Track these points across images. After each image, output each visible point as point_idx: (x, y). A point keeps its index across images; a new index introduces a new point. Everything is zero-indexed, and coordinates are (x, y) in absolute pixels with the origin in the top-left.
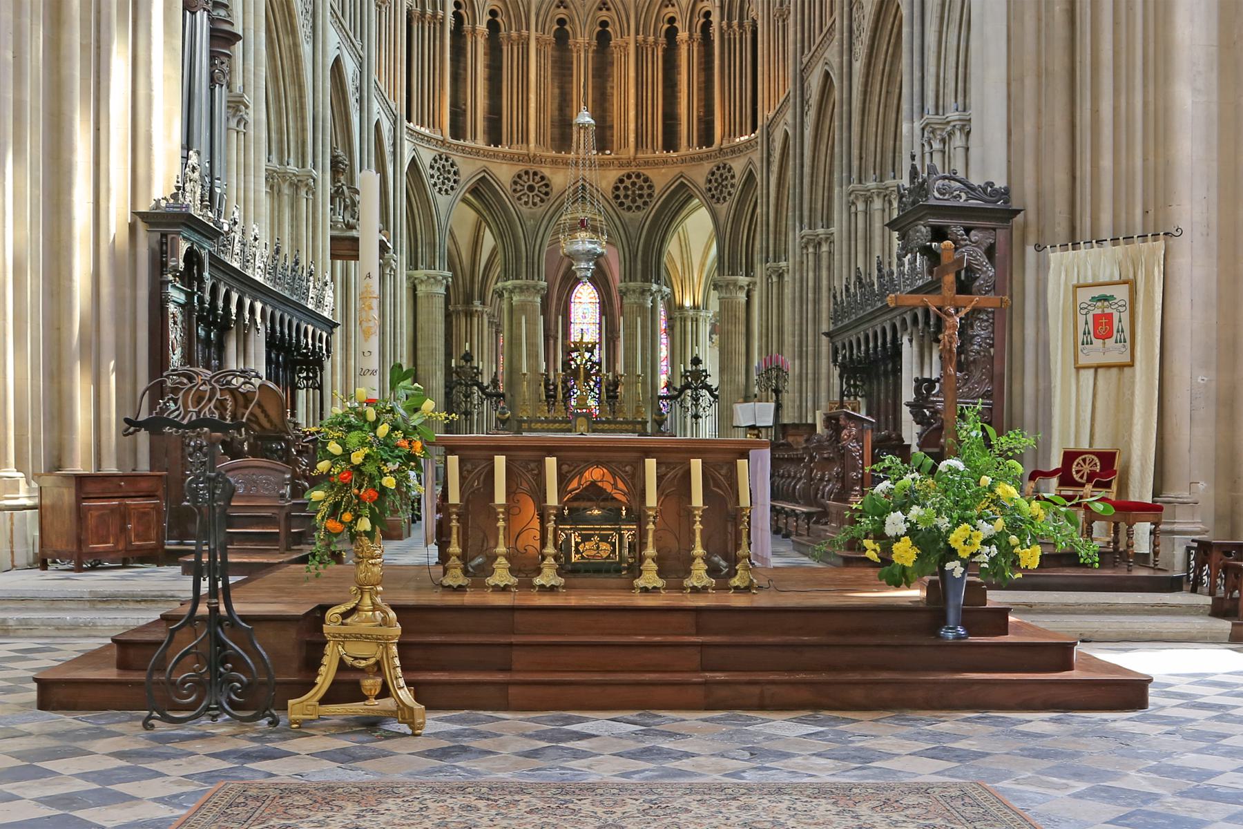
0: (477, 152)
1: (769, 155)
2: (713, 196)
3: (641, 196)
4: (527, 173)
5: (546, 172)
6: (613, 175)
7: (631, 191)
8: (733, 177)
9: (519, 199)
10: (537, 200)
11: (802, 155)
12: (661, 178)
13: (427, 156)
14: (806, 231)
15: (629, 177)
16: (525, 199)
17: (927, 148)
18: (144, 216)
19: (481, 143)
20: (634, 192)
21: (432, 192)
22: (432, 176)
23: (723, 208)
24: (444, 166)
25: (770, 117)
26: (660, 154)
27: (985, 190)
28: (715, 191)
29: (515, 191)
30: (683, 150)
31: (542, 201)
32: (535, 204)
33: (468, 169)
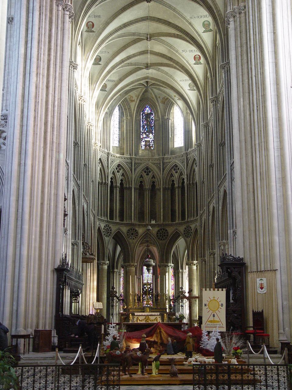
0: (117, 223)
1: (201, 225)
2: (186, 236)
3: (165, 236)
4: (131, 229)
5: (137, 229)
6: (156, 229)
7: (162, 234)
8: (191, 230)
9: (129, 237)
10: (134, 237)
11: (209, 228)
12: (170, 230)
13: (103, 226)
14: (211, 251)
15: (161, 230)
16: (130, 237)
17: (234, 237)
18: (55, 269)
19: (118, 221)
20: (163, 234)
21: (104, 237)
22: (104, 232)
23: (189, 239)
24: (107, 228)
25: (201, 213)
26: (170, 223)
27: (238, 258)
28: (187, 234)
29: (128, 235)
30: (177, 221)
31: (136, 238)
32: (133, 239)
33: (114, 229)
